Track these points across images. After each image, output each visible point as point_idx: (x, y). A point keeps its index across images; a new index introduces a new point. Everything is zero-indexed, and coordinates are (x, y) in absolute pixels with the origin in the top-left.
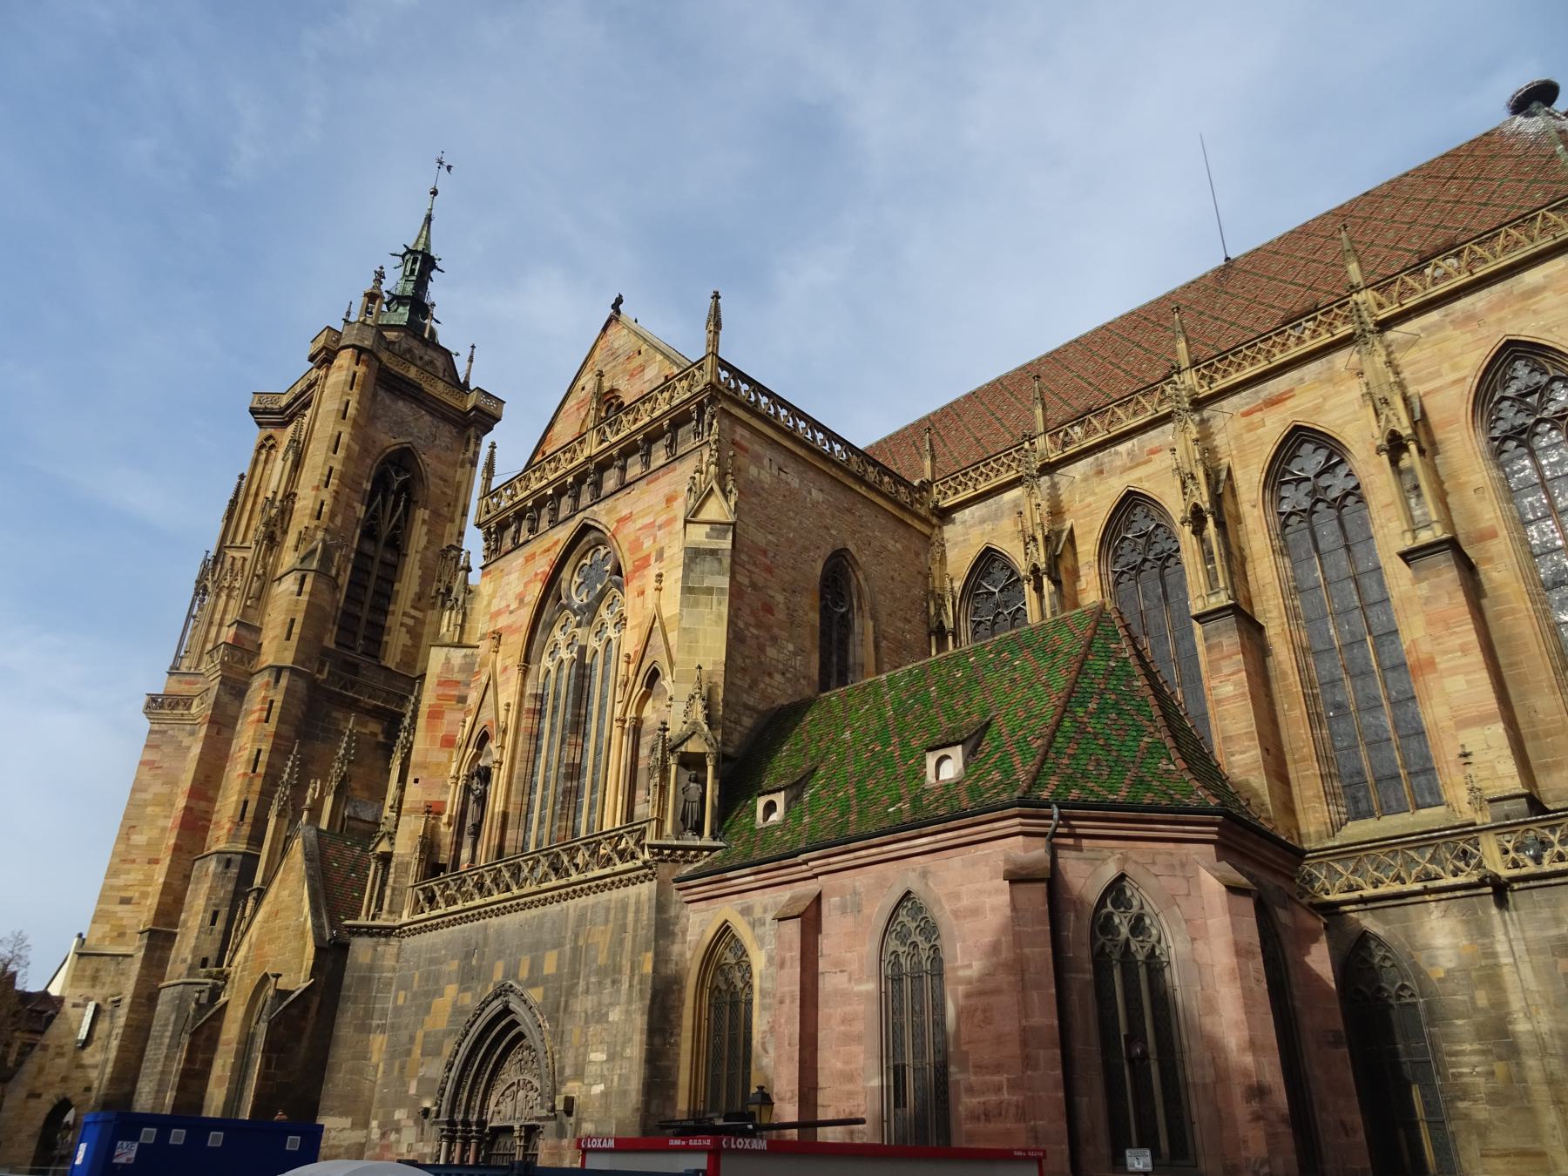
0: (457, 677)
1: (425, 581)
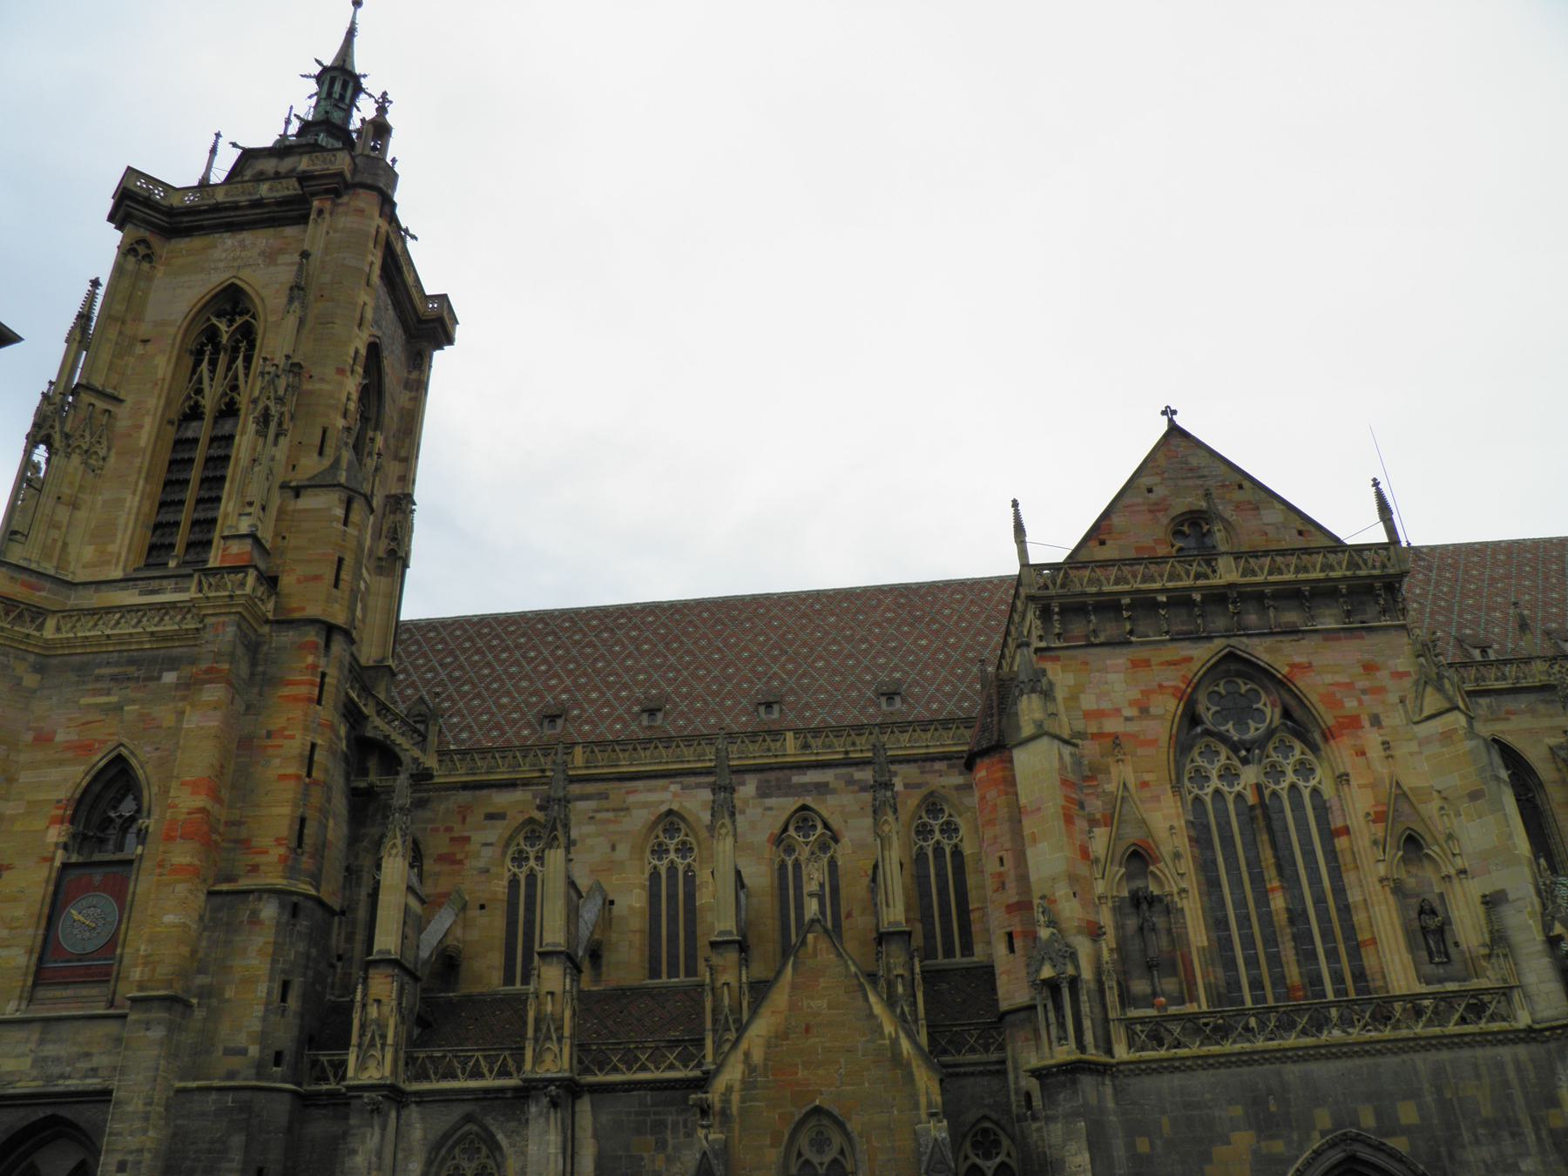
0: (1071, 777)
1: (377, 535)
